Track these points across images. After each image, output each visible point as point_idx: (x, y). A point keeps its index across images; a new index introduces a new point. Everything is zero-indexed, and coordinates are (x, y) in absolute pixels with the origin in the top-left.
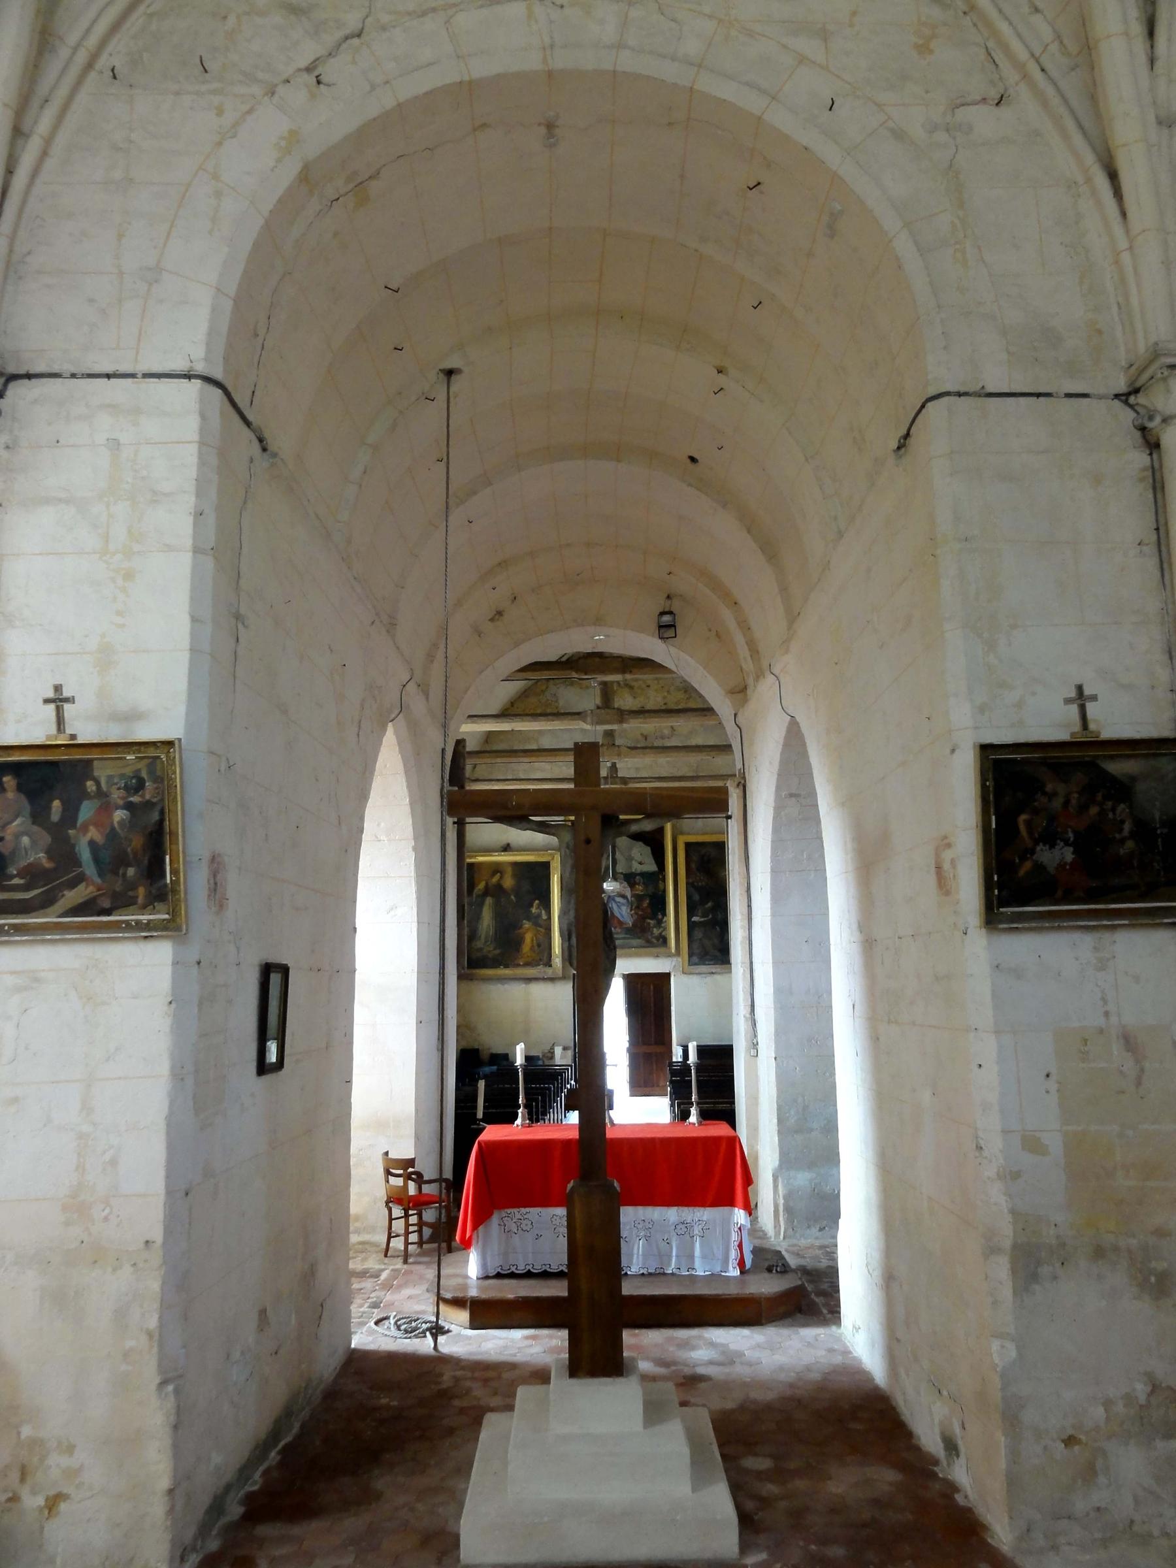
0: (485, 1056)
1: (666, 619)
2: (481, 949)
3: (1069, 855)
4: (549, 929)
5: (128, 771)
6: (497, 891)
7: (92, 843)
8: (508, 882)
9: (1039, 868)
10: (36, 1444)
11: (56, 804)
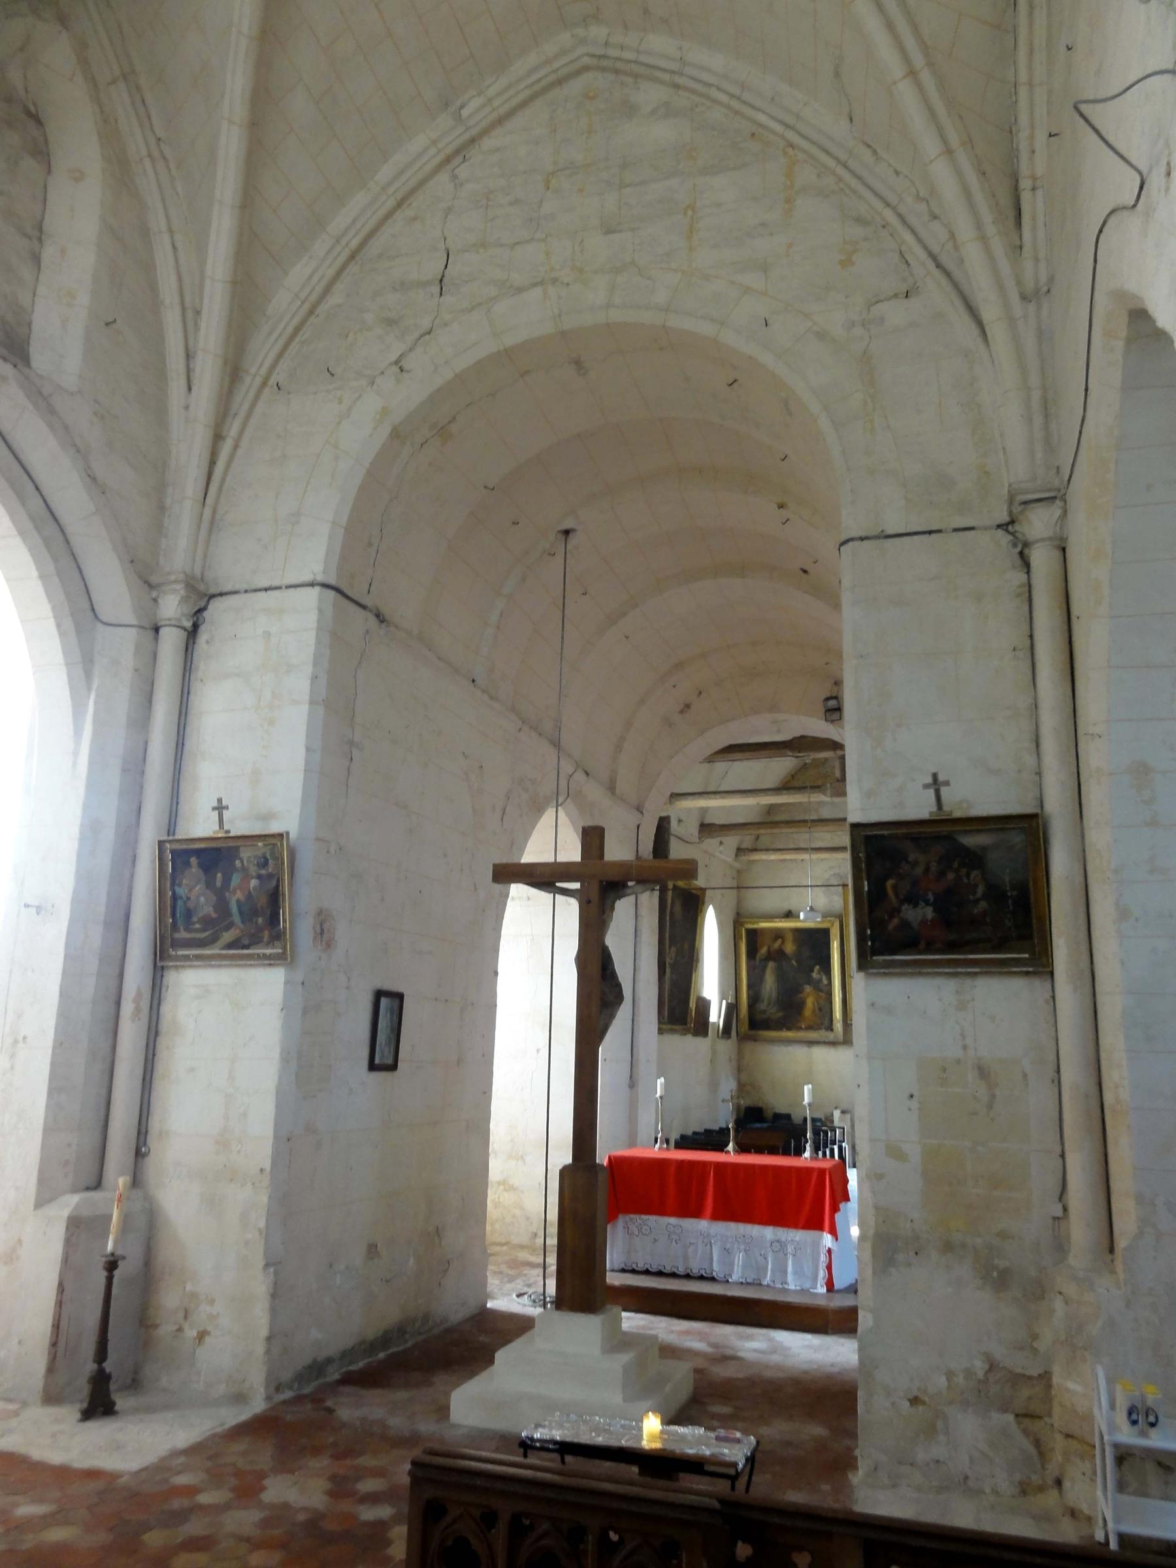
0: (769, 1114)
1: (832, 703)
2: (765, 1012)
3: (929, 913)
5: (259, 853)
6: (778, 955)
7: (238, 901)
8: (790, 948)
9: (905, 924)
10: (194, 1296)
11: (219, 875)
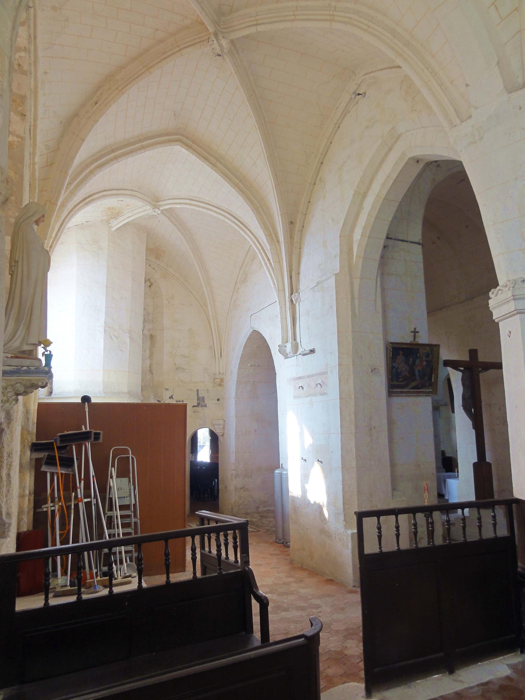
7: (419, 371)
11: (411, 359)
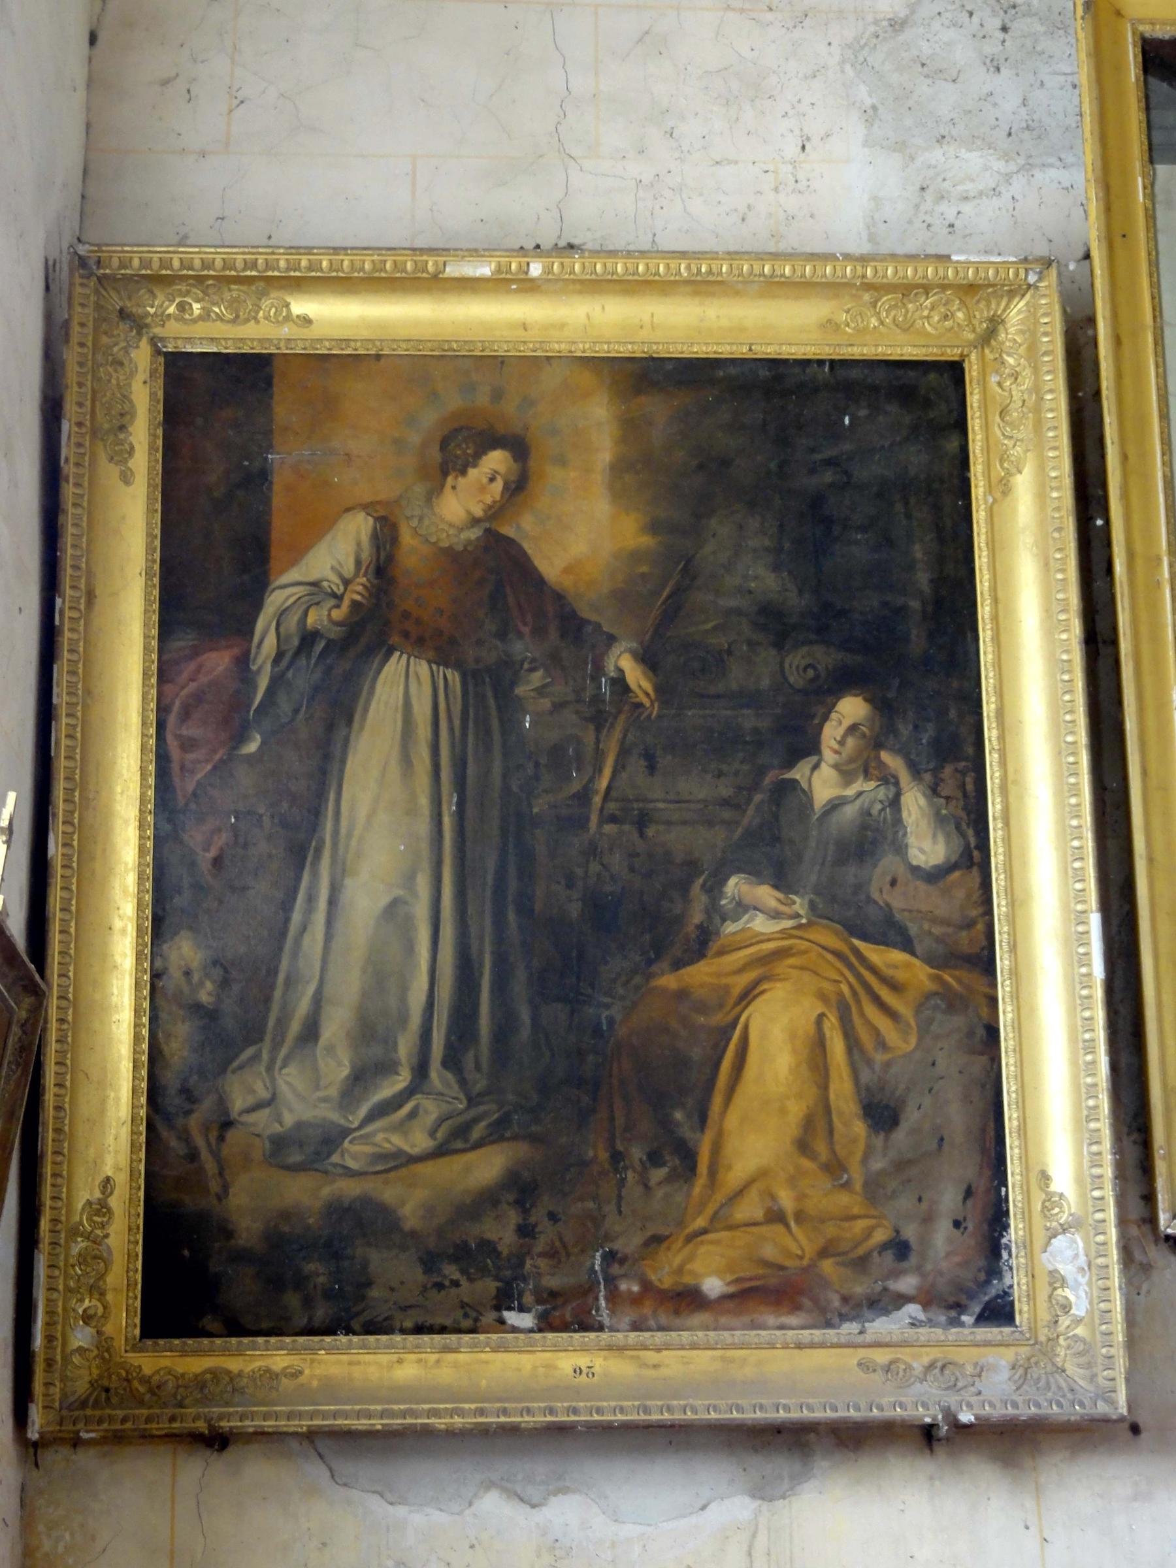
2: (315, 1148)
4: (971, 959)
8: (586, 532)
